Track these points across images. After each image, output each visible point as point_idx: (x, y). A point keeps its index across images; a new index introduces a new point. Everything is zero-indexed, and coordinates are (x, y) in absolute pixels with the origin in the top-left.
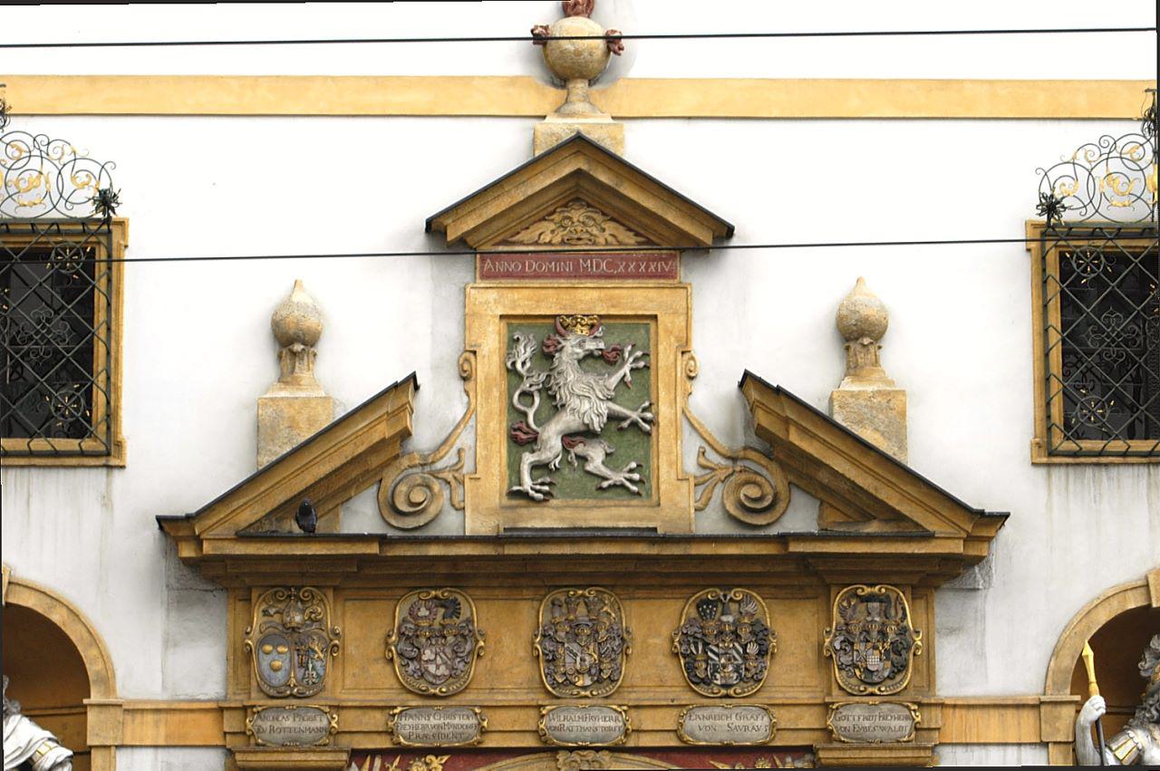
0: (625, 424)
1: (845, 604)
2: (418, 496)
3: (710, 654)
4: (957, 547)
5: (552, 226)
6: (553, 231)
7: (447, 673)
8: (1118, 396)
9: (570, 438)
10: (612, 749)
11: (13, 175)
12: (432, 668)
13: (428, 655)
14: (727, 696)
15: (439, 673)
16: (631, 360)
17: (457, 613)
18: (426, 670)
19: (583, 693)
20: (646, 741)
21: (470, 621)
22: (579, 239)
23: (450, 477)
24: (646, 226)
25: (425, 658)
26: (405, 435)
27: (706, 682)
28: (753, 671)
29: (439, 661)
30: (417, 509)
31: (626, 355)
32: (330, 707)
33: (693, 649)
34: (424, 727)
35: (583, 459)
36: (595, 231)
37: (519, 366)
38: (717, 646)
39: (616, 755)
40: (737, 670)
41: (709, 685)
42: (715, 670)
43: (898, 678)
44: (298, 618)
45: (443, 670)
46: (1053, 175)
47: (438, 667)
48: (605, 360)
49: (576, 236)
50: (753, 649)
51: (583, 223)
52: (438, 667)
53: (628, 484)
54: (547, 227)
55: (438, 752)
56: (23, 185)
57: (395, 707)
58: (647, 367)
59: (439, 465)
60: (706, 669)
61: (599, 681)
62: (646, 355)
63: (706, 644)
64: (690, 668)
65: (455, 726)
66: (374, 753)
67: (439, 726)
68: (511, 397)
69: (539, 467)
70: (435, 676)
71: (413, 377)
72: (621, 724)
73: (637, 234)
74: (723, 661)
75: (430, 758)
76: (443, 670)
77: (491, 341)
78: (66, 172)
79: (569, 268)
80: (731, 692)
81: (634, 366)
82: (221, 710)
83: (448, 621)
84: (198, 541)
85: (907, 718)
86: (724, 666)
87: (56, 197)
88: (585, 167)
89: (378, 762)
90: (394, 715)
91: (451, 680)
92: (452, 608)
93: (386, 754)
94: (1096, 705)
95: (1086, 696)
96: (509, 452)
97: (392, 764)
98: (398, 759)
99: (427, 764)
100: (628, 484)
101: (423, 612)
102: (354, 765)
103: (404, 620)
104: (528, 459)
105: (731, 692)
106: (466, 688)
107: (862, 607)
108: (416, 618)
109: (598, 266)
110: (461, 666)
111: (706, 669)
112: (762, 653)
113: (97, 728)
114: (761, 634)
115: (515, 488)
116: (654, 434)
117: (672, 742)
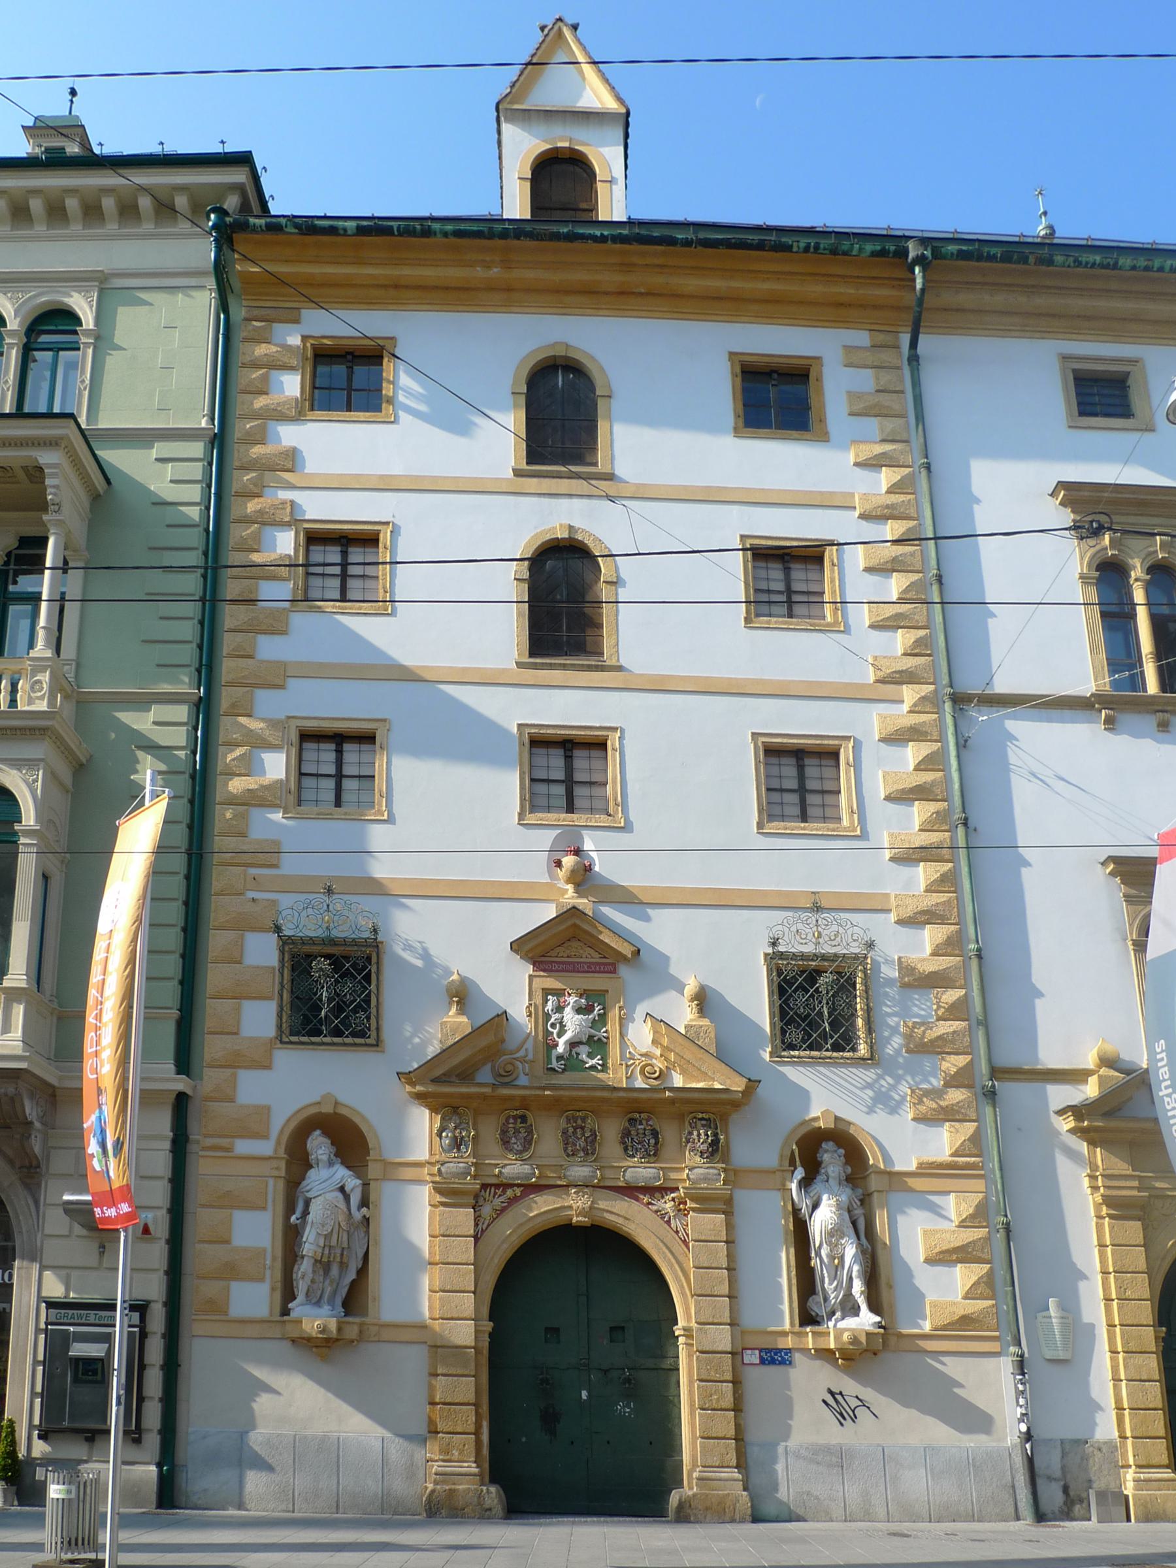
2: (509, 1068)
8: (804, 1029)
13: (514, 1140)
26: (503, 1041)
30: (509, 1073)
45: (520, 1148)
46: (774, 930)
50: (652, 1141)
59: (517, 1055)
64: (626, 1149)
66: (491, 1185)
76: (520, 1148)
92: (524, 1119)
93: (497, 1186)
101: (511, 1121)
112: (656, 1143)
113: (373, 1170)
114: (655, 1134)
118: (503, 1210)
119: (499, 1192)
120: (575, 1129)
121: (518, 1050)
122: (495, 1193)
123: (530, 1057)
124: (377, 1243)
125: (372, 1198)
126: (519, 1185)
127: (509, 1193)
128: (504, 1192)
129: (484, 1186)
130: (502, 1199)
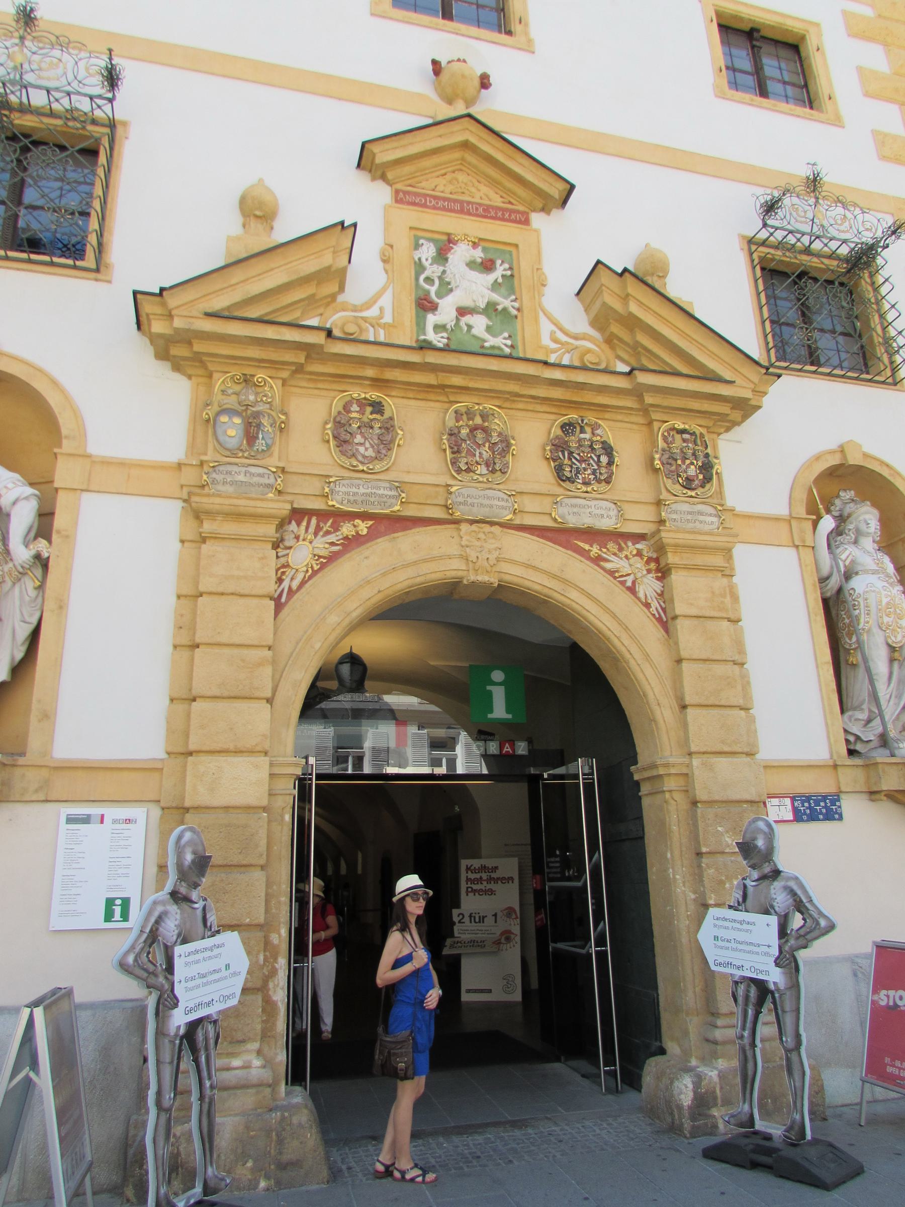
0: (500, 308)
1: (666, 434)
3: (574, 460)
4: (748, 394)
5: (444, 182)
6: (445, 186)
7: (373, 455)
9: (462, 312)
10: (502, 525)
11: (36, 58)
12: (362, 449)
13: (359, 439)
14: (587, 492)
15: (367, 454)
16: (502, 268)
17: (381, 412)
18: (357, 450)
19: (481, 479)
20: (529, 521)
21: (391, 419)
22: (463, 193)
23: (374, 322)
24: (509, 190)
25: (356, 441)
27: (570, 480)
28: (606, 476)
29: (367, 445)
31: (498, 265)
32: (277, 467)
33: (561, 456)
34: (355, 494)
35: (470, 327)
36: (473, 190)
37: (423, 260)
38: (579, 454)
39: (505, 530)
40: (594, 473)
41: (573, 482)
42: (578, 471)
43: (708, 486)
44: (252, 398)
45: (370, 453)
47: (366, 449)
48: (487, 266)
49: (460, 190)
50: (604, 459)
51: (466, 184)
52: (366, 449)
53: (503, 347)
54: (442, 181)
55: (364, 516)
56: (44, 65)
57: (331, 477)
58: (512, 276)
59: (365, 314)
60: (571, 471)
61: (493, 471)
62: (511, 268)
63: (571, 453)
64: (559, 470)
65: (381, 496)
67: (367, 494)
68: (417, 279)
69: (438, 328)
70: (364, 457)
71: (355, 225)
72: (510, 505)
73: (501, 197)
74: (583, 466)
75: (358, 522)
76: (370, 453)
77: (403, 242)
78: (82, 64)
79: (458, 207)
80: (589, 489)
81: (504, 273)
82: (180, 466)
83: (374, 416)
84: (170, 316)
85: (715, 516)
86: (585, 469)
87: (71, 77)
88: (473, 140)
89: (314, 521)
90: (330, 483)
91: (376, 462)
92: (377, 407)
93: (322, 515)
94: (827, 523)
95: (820, 517)
96: (417, 316)
97: (325, 524)
98: (331, 521)
99: (355, 526)
100: (503, 347)
101: (355, 407)
102: (293, 523)
103: (339, 413)
104: (431, 319)
105: (589, 489)
106: (387, 470)
107: (678, 437)
108: (349, 412)
109: (477, 209)
110: (384, 452)
111: (571, 471)
113: (65, 474)
114: (608, 450)
115: (422, 337)
116: (519, 318)
117: (548, 523)
118: (332, 558)
119: (327, 526)
120: (473, 429)
121: (368, 305)
122: (318, 529)
123: (388, 319)
124: (62, 606)
125: (59, 522)
126: (364, 516)
127: (347, 529)
128: (336, 528)
129: (298, 514)
130: (332, 538)
